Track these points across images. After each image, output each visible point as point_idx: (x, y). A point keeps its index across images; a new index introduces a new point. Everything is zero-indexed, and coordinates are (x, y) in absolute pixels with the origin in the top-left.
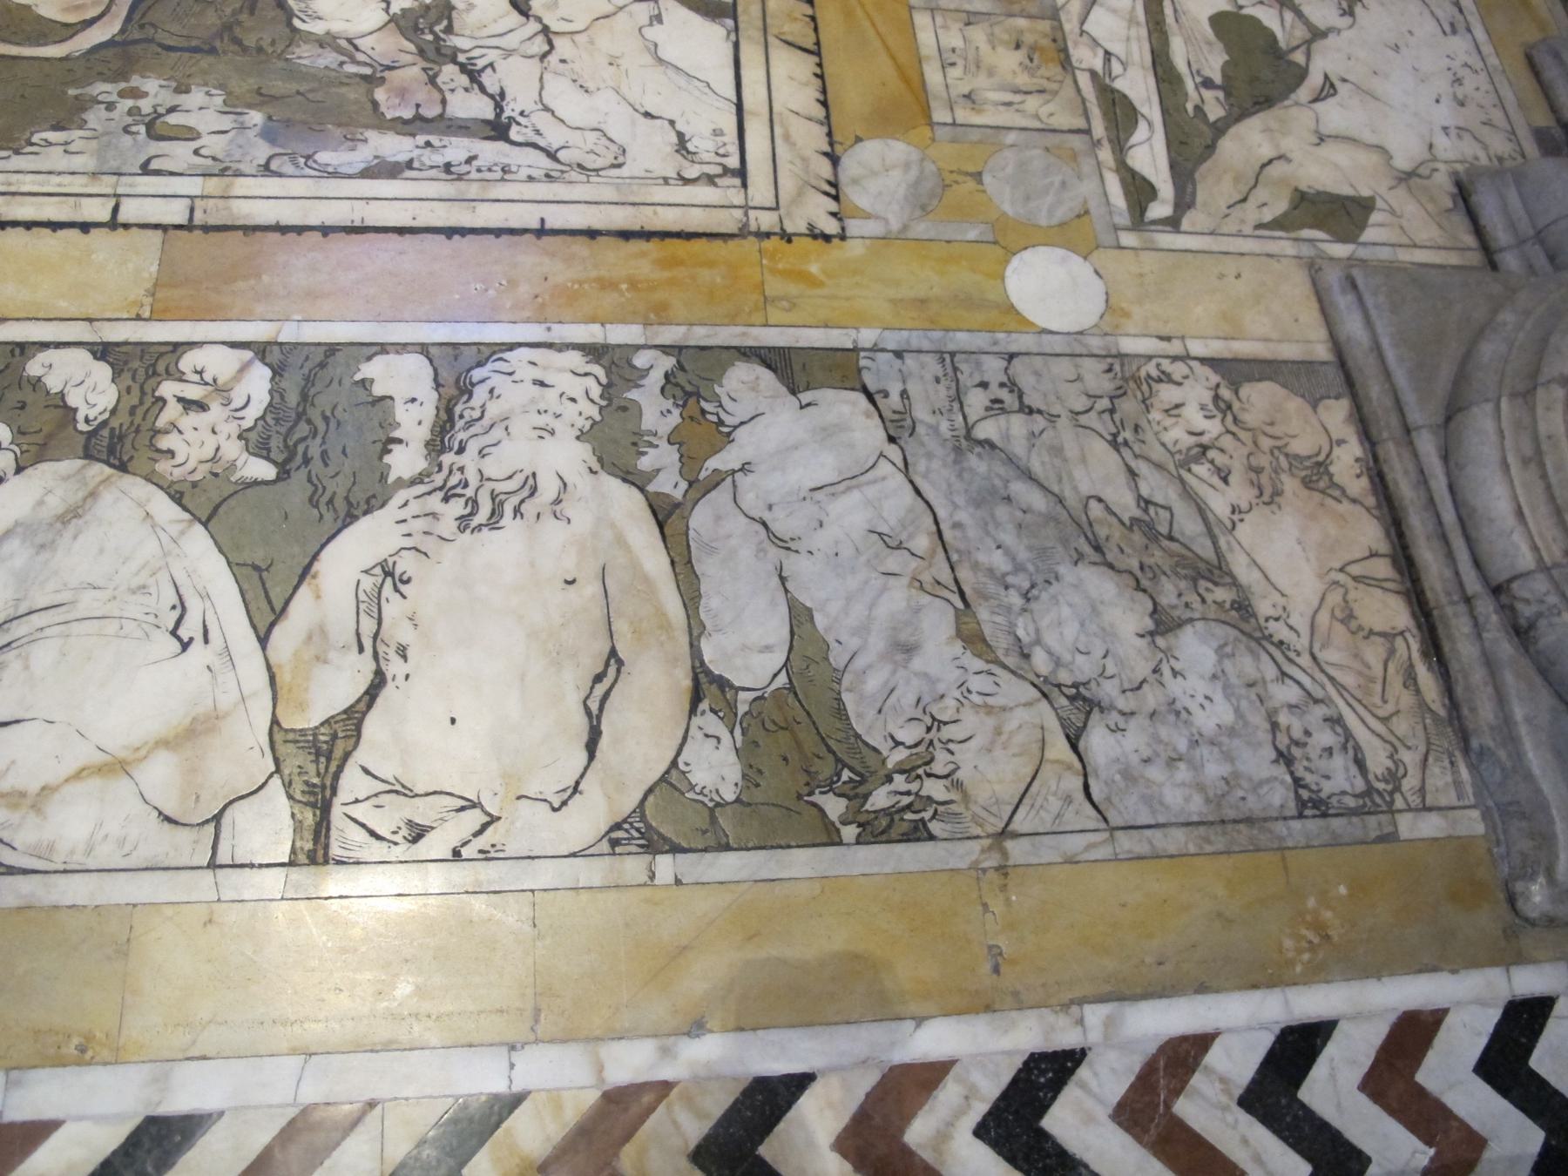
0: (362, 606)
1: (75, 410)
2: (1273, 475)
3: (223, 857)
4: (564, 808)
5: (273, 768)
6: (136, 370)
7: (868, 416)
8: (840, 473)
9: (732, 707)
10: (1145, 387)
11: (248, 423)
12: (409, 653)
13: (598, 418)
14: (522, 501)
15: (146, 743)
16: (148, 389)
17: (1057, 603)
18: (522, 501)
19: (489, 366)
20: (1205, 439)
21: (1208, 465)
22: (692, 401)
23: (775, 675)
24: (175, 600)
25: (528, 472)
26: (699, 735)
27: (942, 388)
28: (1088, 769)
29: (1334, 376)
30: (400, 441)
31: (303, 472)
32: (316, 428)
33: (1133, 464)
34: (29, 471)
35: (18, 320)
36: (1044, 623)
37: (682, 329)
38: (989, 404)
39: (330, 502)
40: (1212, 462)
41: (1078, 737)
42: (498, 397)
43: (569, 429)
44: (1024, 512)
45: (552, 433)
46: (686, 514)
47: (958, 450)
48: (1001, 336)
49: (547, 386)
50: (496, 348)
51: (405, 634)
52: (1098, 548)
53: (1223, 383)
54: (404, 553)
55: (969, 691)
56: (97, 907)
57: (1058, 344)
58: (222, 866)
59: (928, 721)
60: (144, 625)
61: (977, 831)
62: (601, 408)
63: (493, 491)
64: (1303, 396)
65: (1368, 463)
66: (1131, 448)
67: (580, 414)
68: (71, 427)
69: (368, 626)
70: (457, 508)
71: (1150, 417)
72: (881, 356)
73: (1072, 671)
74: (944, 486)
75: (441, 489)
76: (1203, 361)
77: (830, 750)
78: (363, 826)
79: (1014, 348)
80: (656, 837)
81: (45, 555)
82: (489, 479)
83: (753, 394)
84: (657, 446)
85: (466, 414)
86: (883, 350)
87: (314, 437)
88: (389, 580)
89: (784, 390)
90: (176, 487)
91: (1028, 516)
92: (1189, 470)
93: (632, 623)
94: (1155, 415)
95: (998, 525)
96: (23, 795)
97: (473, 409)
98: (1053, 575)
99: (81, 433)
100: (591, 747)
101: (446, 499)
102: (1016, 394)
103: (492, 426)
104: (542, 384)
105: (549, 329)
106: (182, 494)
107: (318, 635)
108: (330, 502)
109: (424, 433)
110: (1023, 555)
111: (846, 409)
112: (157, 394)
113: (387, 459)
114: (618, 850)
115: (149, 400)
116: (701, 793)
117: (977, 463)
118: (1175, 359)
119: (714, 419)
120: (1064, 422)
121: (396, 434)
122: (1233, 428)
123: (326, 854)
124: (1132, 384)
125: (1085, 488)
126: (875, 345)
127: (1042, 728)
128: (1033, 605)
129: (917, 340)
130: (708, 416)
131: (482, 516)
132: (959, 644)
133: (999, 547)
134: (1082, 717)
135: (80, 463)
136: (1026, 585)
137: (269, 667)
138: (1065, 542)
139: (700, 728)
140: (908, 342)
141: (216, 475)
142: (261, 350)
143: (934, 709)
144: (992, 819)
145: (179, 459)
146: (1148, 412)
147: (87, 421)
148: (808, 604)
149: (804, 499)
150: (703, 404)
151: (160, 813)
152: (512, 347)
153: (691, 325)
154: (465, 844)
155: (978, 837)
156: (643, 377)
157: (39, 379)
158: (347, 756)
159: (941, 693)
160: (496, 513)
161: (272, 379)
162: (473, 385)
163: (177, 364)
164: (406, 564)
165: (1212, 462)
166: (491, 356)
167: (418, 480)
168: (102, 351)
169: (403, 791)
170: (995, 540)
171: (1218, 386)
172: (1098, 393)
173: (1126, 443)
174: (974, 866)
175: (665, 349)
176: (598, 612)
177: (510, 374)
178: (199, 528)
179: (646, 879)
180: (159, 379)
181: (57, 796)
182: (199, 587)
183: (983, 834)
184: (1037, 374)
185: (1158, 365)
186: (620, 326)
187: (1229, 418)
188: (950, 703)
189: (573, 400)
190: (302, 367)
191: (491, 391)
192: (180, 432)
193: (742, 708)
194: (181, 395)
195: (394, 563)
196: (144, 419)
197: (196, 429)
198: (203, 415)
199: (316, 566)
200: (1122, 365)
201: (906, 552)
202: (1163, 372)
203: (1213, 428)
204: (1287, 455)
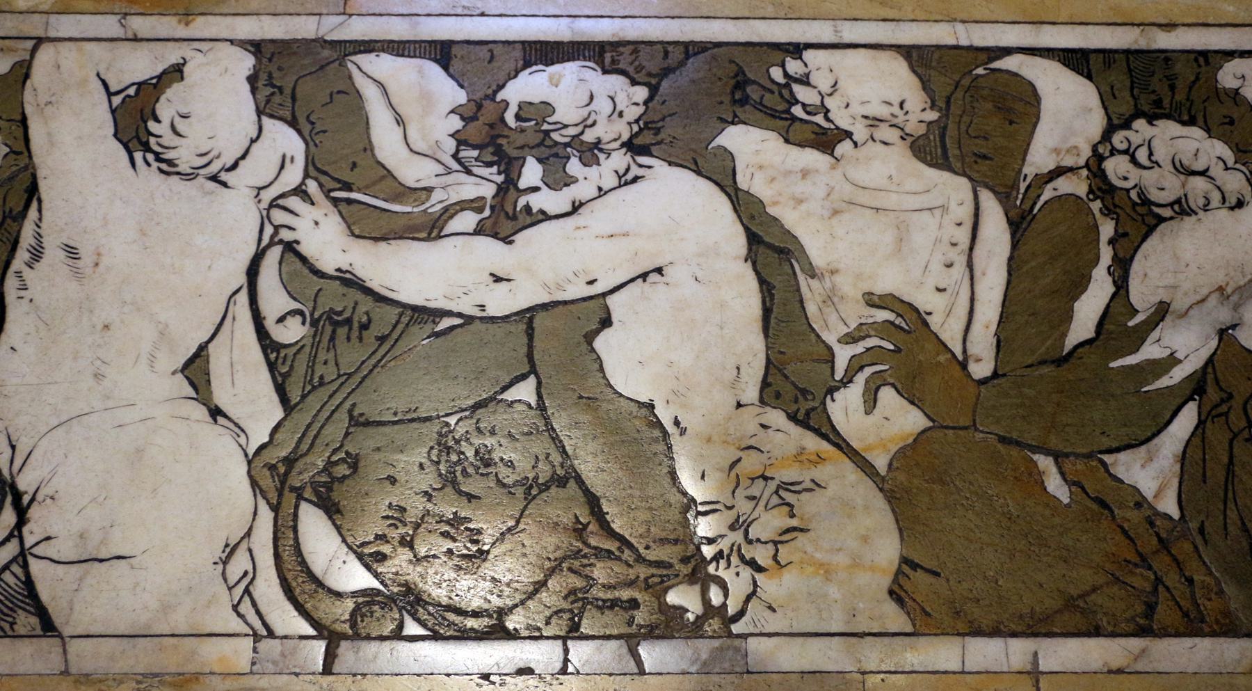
35: (1189, 25)
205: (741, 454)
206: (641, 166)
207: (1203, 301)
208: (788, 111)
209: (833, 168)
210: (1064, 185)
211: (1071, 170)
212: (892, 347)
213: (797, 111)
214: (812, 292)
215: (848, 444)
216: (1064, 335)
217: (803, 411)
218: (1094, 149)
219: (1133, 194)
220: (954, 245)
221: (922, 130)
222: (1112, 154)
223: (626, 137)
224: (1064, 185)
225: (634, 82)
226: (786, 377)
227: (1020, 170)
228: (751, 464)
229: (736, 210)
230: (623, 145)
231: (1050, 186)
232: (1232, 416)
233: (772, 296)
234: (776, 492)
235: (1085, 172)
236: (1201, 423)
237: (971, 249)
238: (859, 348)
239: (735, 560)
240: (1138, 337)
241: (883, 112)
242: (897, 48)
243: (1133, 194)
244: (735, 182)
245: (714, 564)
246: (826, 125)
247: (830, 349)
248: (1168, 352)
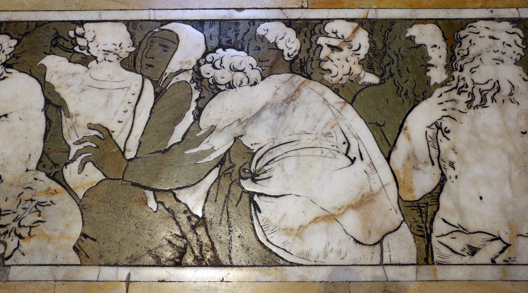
0: (430, 143)
1: (283, 51)
3: (386, 260)
5: (402, 219)
6: (306, 32)
11: (362, 57)
12: (456, 165)
13: (523, 54)
14: (495, 94)
15: (343, 206)
16: (313, 40)
19: (467, 30)
24: (344, 140)
25: (495, 80)
30: (432, 66)
31: (391, 80)
32: (393, 60)
34: (267, 79)
35: (249, 9)
39: (406, 94)
42: (474, 44)
43: (510, 59)
49: (496, 39)
50: (469, 21)
51: (452, 157)
54: (444, 118)
56: (333, 282)
58: (386, 265)
60: (333, 151)
63: (480, 89)
67: (514, 52)
68: (282, 59)
69: (434, 152)
70: (464, 97)
75: (456, 88)
78: (447, 247)
81: (282, 118)
82: (477, 84)
85: (461, 52)
87: (393, 63)
88: (440, 131)
90: (335, 86)
96: (292, 230)
97: (463, 50)
99: (287, 61)
101: (459, 93)
103: (474, 58)
105: (492, 11)
106: (338, 90)
107: (412, 157)
108: (406, 94)
109: (442, 62)
112: (318, 43)
113: (428, 74)
115: (314, 47)
121: (430, 62)
123: (433, 260)
131: (477, 101)
135: (289, 75)
137: (392, 172)
141: (352, 81)
142: (362, 23)
145: (334, 74)
147: (289, 55)
151: (355, 239)
152: (475, 20)
154: (497, 257)
157: (264, 36)
158: (435, 213)
160: (484, 100)
161: (369, 36)
162: (461, 39)
163: (324, 28)
164: (446, 123)
166: (467, 25)
167: (443, 84)
168: (289, 23)
169: (462, 230)
177: (478, 33)
178: (349, 106)
180: (317, 36)
181: (307, 231)
182: (354, 133)
190: (381, 31)
191: (470, 41)
192: (332, 61)
194: (329, 43)
195: (441, 123)
196: (314, 55)
197: (339, 60)
198: (341, 53)
199: (405, 125)
205: (24, 190)
206: (7, 73)
207: (231, 125)
208: (73, 49)
209: (86, 72)
210: (182, 77)
211: (186, 70)
212: (95, 146)
213: (77, 49)
214: (66, 123)
215: (69, 187)
216: (168, 140)
217: (53, 173)
218: (198, 61)
219: (210, 81)
220: (129, 103)
221: (127, 55)
222: (205, 63)
223: (3, 61)
224: (182, 77)
225: (12, 38)
226: (49, 158)
227: (164, 71)
228: (28, 194)
229: (42, 90)
230: (2, 64)
231: (175, 78)
232: (233, 174)
233: (50, 125)
234: (35, 206)
235: (191, 71)
236: (219, 177)
237: (136, 105)
238: (81, 147)
239: (13, 234)
240: (199, 142)
241: (111, 48)
242: (124, 21)
243: (210, 81)
244: (45, 79)
245: (4, 236)
246: (87, 54)
247: (69, 147)
248: (211, 147)
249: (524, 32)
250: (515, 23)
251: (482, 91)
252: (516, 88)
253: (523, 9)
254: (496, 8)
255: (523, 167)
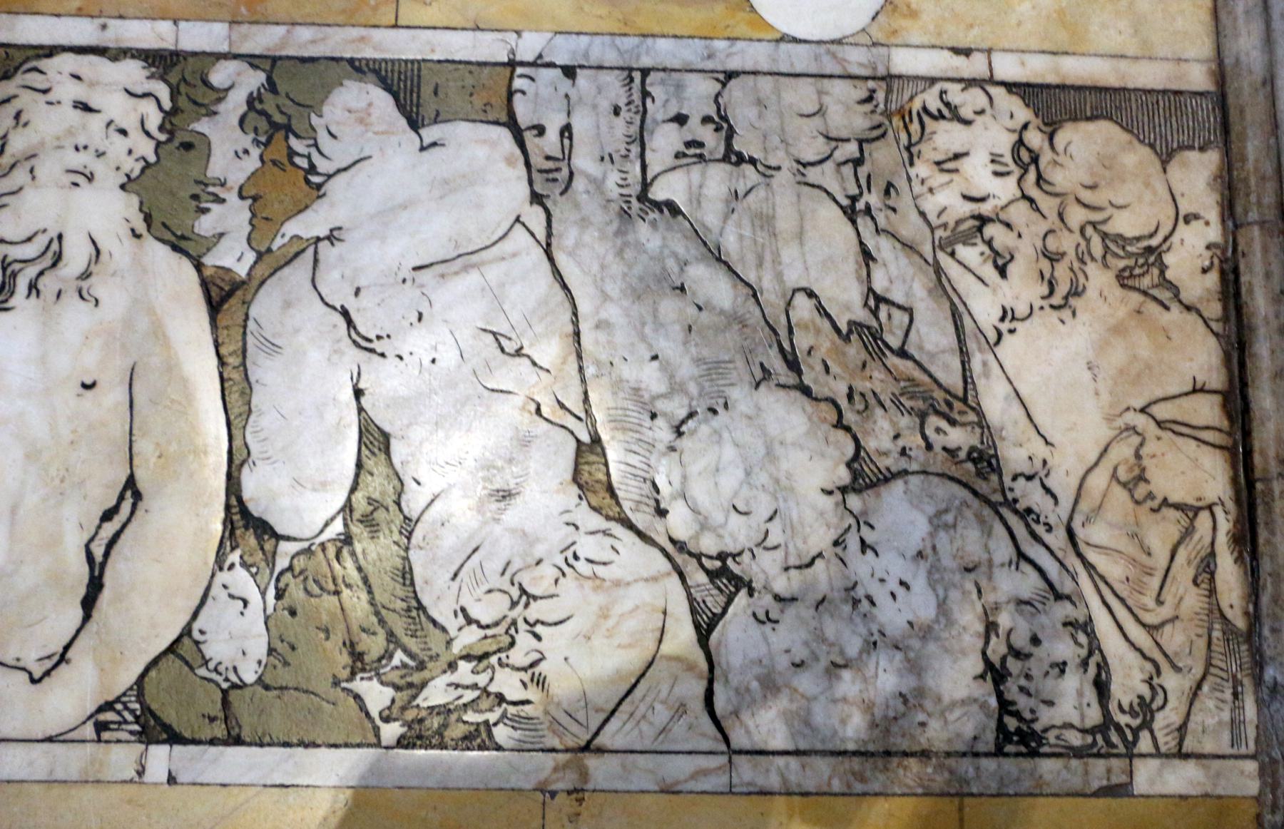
2: (1076, 265)
4: (46, 680)
7: (510, 161)
8: (457, 246)
9: (271, 559)
10: (915, 127)
13: (152, 159)
14: (41, 273)
17: (719, 441)
18: (41, 273)
19: (19, 79)
20: (986, 209)
21: (983, 248)
22: (280, 135)
23: (327, 525)
26: (223, 595)
27: (619, 123)
28: (717, 672)
29: (1206, 112)
33: (870, 244)
36: (694, 469)
37: (281, 30)
38: (682, 148)
40: (989, 243)
41: (711, 627)
42: (26, 125)
43: (113, 173)
44: (700, 308)
45: (90, 178)
46: (248, 297)
47: (625, 214)
48: (720, 45)
50: (30, 53)
52: (793, 364)
53: (1036, 122)
55: (576, 557)
57: (800, 59)
59: (515, 592)
61: (556, 743)
62: (159, 144)
63: (5, 257)
64: (1152, 146)
65: (1224, 251)
66: (873, 218)
67: (130, 152)
71: (912, 172)
72: (546, 75)
73: (720, 536)
74: (595, 268)
76: (1010, 87)
77: (382, 622)
79: (733, 65)
80: (152, 722)
83: (360, 129)
84: (223, 201)
86: (551, 65)
89: (403, 122)
91: (704, 315)
92: (952, 254)
93: (157, 444)
94: (922, 169)
95: (659, 325)
98: (721, 401)
100: (89, 603)
102: (724, 133)
103: (13, 166)
104: (85, 108)
110: (686, 369)
111: (481, 152)
114: (106, 735)
116: (216, 670)
117: (648, 235)
118: (969, 83)
119: (304, 163)
120: (784, 178)
122: (1034, 192)
124: (897, 121)
125: (794, 277)
126: (540, 56)
127: (665, 613)
128: (685, 443)
129: (602, 51)
130: (298, 160)
132: (575, 490)
133: (655, 358)
134: (722, 600)
136: (683, 413)
138: (747, 355)
139: (225, 587)
140: (586, 55)
143: (525, 579)
144: (574, 728)
146: (912, 164)
148: (387, 428)
149: (404, 281)
150: (293, 142)
152: (51, 51)
153: (294, 24)
155: (553, 750)
156: (220, 100)
159: (537, 555)
165: (989, 243)
170: (650, 346)
171: (1025, 126)
172: (844, 135)
173: (868, 210)
174: (541, 789)
175: (253, 60)
176: (118, 428)
177: (45, 92)
179: (134, 774)
183: (559, 746)
184: (760, 103)
185: (943, 93)
186: (199, 24)
187: (1032, 176)
188: (548, 572)
189: (123, 132)
191: (18, 116)
193: (282, 563)
200: (889, 91)
201: (526, 361)
202: (947, 105)
203: (1004, 190)
204: (1104, 236)
249: (174, 94)
250: (158, 68)
251: (10, 264)
252: (104, 257)
253: (191, 24)
254: (121, 17)
255: (57, 482)
